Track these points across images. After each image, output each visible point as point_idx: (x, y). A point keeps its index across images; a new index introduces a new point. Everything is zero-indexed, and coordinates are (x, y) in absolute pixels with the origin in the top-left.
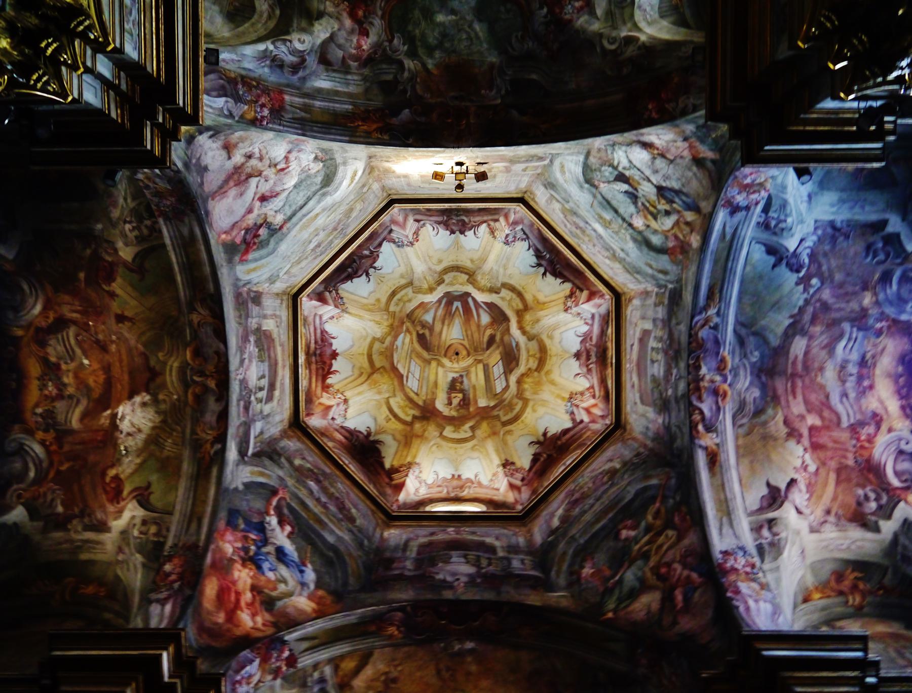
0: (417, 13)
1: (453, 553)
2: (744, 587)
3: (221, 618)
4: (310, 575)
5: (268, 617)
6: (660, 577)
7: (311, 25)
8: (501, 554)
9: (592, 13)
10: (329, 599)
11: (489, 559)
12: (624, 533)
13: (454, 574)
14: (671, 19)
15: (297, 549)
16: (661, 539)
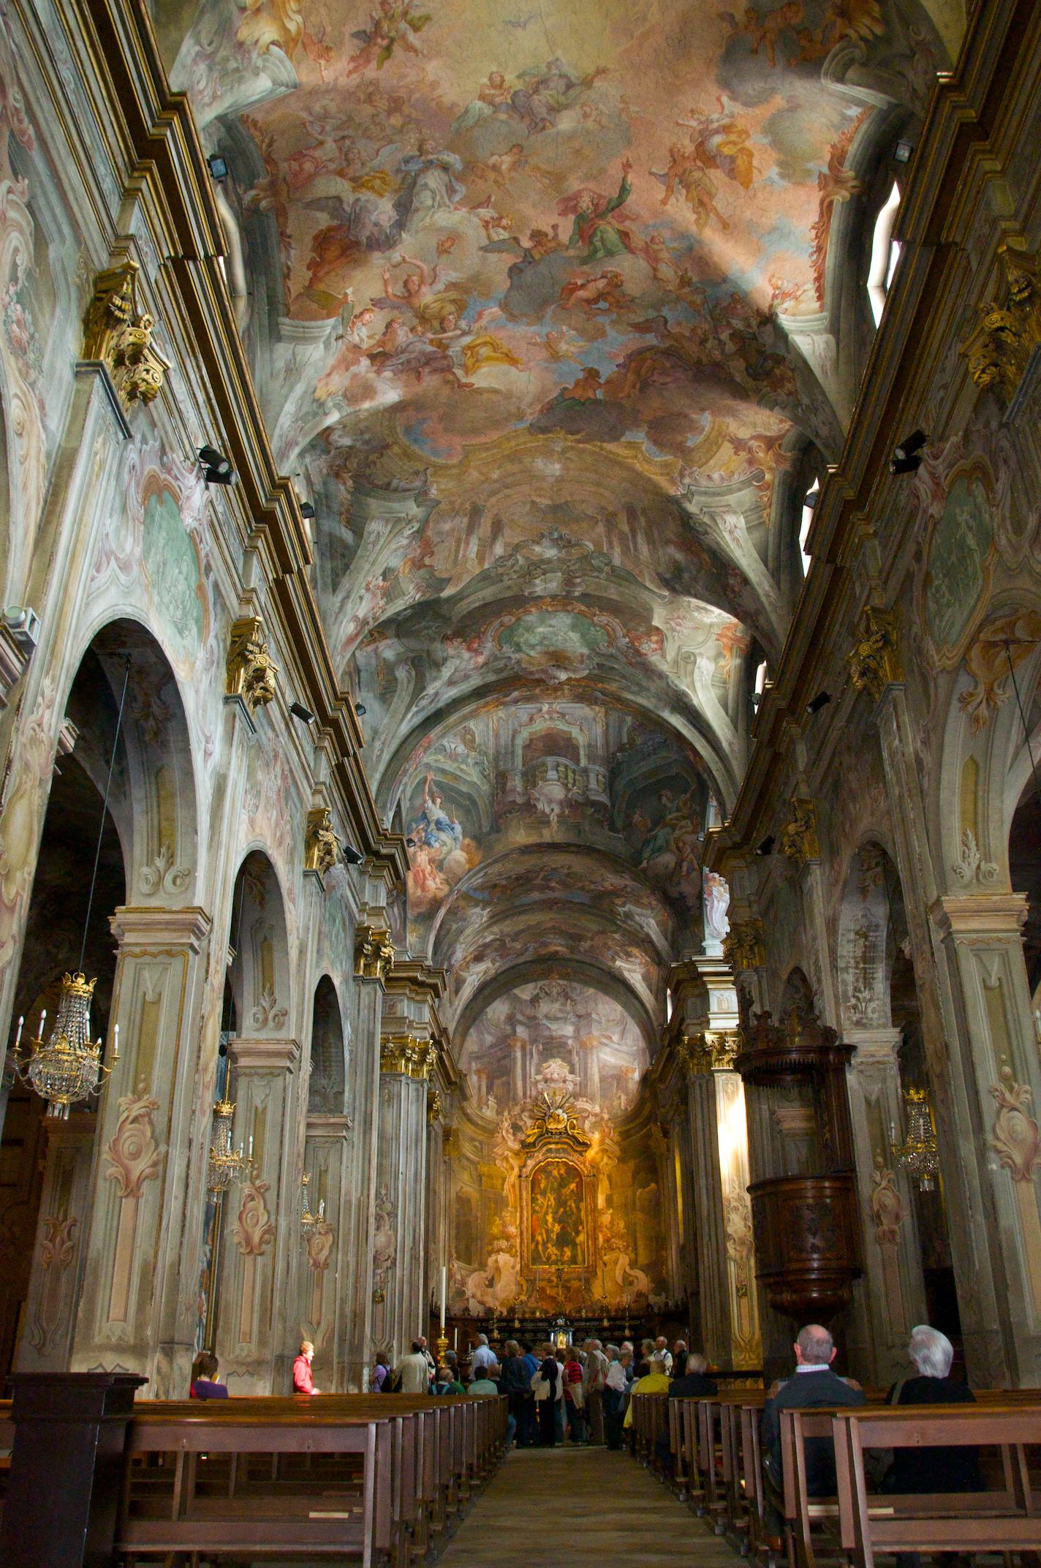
0: (521, 630)
1: (550, 760)
2: (715, 893)
3: (419, 892)
4: (458, 828)
5: (442, 875)
6: (678, 848)
7: (439, 671)
8: (583, 762)
9: (664, 656)
10: (473, 844)
11: (574, 772)
12: (664, 800)
13: (550, 801)
14: (720, 692)
15: (447, 814)
16: (683, 823)
